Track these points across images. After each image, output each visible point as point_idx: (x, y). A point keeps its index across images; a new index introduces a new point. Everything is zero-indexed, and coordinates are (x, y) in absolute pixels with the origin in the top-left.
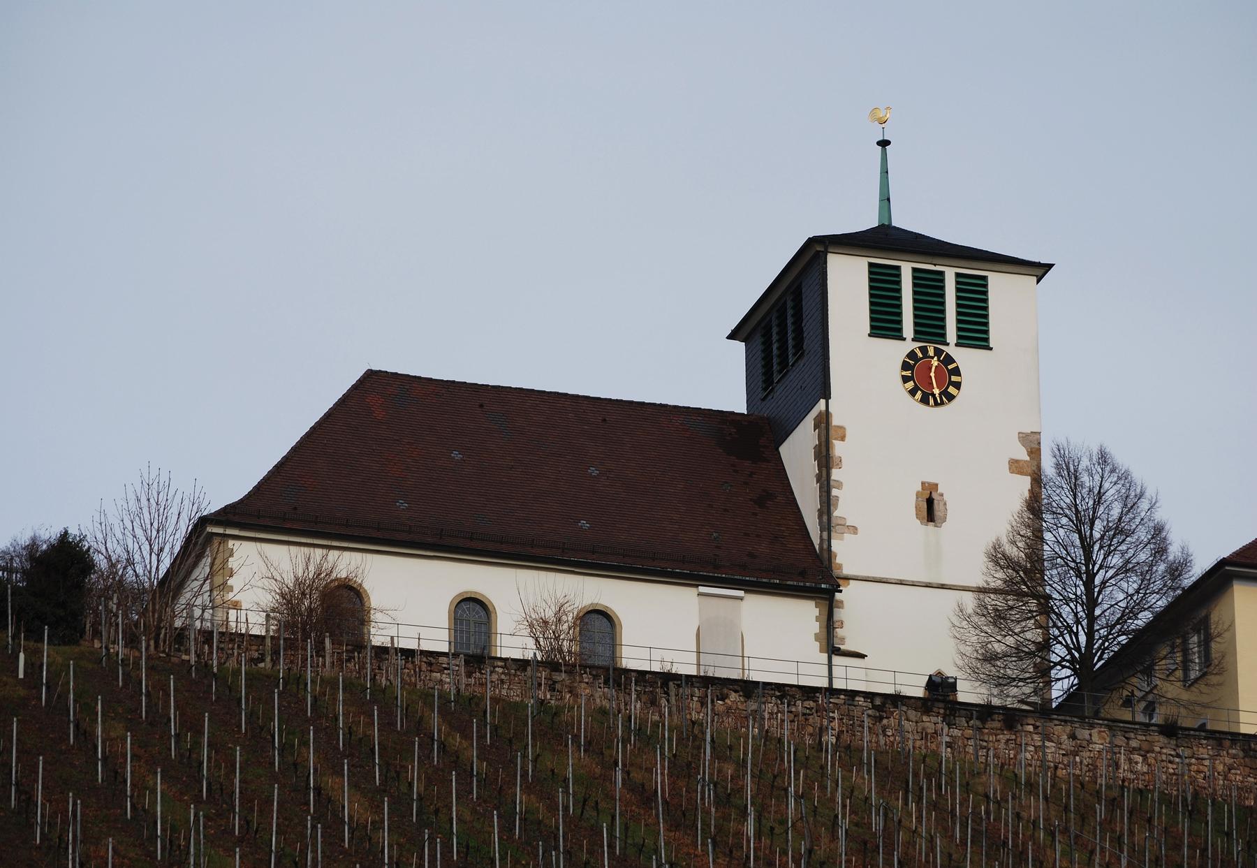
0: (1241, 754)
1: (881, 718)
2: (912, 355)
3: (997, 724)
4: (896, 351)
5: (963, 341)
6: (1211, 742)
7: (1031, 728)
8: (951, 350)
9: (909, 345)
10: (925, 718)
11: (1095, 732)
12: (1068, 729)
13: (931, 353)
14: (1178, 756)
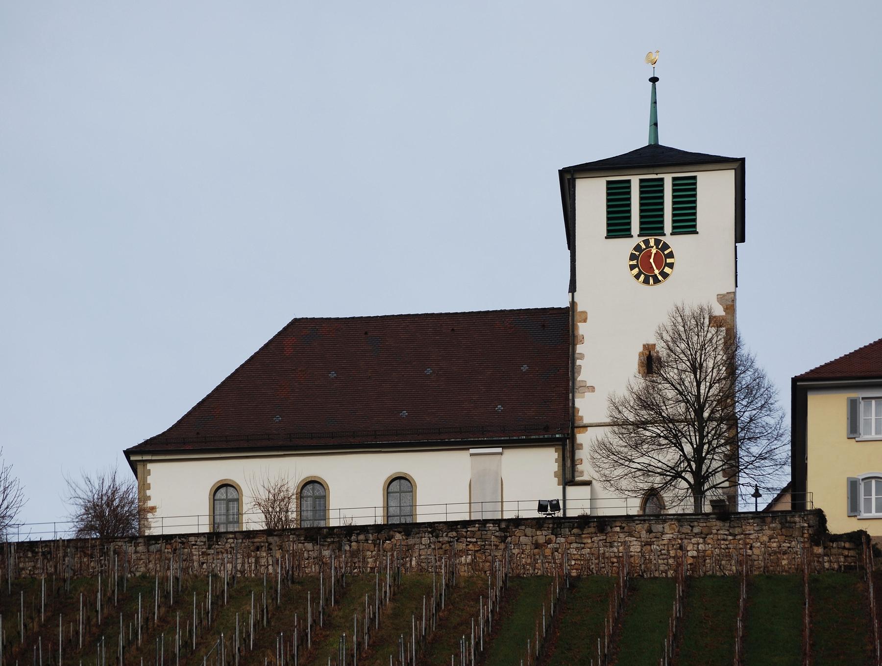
0: (779, 526)
1: (506, 537)
2: (638, 248)
3: (592, 530)
4: (626, 246)
5: (677, 230)
6: (757, 520)
7: (618, 529)
8: (668, 239)
9: (636, 240)
10: (538, 533)
11: (667, 526)
12: (646, 525)
13: (652, 243)
14: (730, 534)
